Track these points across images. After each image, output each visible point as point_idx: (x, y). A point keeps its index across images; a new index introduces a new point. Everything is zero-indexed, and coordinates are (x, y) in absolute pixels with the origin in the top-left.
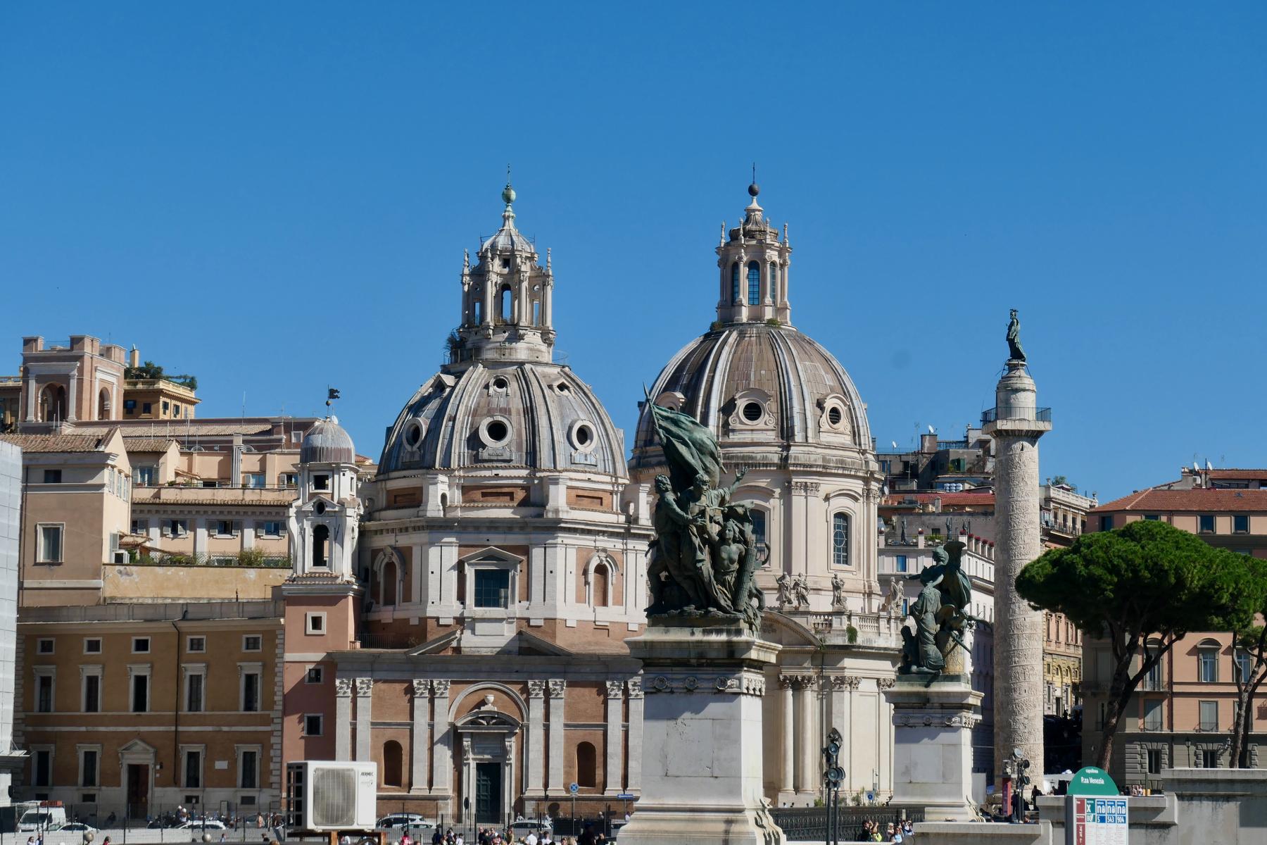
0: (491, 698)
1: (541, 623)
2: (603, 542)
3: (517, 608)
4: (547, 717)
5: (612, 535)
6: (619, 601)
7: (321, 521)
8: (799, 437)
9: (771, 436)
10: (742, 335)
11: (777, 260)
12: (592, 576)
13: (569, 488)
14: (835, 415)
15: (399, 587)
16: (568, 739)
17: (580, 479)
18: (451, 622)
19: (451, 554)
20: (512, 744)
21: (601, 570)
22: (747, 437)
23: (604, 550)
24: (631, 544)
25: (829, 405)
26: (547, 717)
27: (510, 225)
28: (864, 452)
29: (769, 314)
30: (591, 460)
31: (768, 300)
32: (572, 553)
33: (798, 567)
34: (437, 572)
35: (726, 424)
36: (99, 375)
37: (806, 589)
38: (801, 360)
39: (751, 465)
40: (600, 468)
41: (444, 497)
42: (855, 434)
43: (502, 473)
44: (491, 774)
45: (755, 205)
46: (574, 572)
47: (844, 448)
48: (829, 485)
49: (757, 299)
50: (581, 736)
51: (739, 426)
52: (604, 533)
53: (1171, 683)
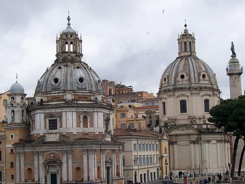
2: (85, 110)
4: (67, 160)
5: (89, 107)
6: (92, 125)
7: (13, 109)
9: (187, 82)
11: (191, 41)
12: (82, 120)
13: (75, 95)
14: (204, 76)
15: (34, 126)
18: (42, 135)
19: (42, 116)
21: (85, 118)
22: (181, 83)
23: (86, 112)
25: (202, 74)
26: (67, 160)
28: (212, 84)
29: (189, 54)
30: (84, 87)
32: (74, 114)
34: (39, 121)
36: (108, 87)
37: (195, 119)
39: (181, 89)
40: (87, 89)
41: (42, 100)
42: (209, 80)
46: (76, 119)
47: (206, 84)
48: (202, 93)
49: (186, 51)
50: (76, 166)
52: (85, 107)
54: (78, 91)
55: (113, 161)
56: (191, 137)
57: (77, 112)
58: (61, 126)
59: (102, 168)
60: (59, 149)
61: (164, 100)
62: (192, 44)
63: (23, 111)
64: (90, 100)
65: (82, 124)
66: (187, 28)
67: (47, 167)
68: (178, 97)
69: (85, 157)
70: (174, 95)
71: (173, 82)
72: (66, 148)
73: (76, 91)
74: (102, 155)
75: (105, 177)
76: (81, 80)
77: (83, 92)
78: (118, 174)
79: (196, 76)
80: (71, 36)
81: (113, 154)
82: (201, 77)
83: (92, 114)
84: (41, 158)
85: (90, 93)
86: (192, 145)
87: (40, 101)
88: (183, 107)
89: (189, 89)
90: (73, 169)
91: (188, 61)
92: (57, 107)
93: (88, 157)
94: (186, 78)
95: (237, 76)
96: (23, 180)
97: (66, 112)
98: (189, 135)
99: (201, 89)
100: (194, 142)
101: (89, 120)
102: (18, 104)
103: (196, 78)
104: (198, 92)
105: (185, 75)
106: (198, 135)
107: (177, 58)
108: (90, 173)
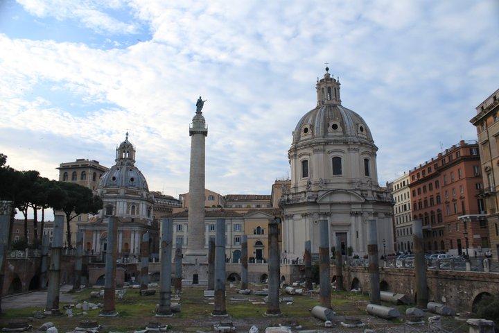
9: (341, 134)
22: (334, 134)
56: (353, 206)
66: (329, 72)
68: (329, 153)
70: (324, 150)
82: (359, 130)
86: (353, 218)
88: (337, 165)
89: (346, 143)
94: (340, 128)
98: (350, 204)
100: (356, 214)
104: (357, 147)
105: (338, 124)
106: (363, 204)
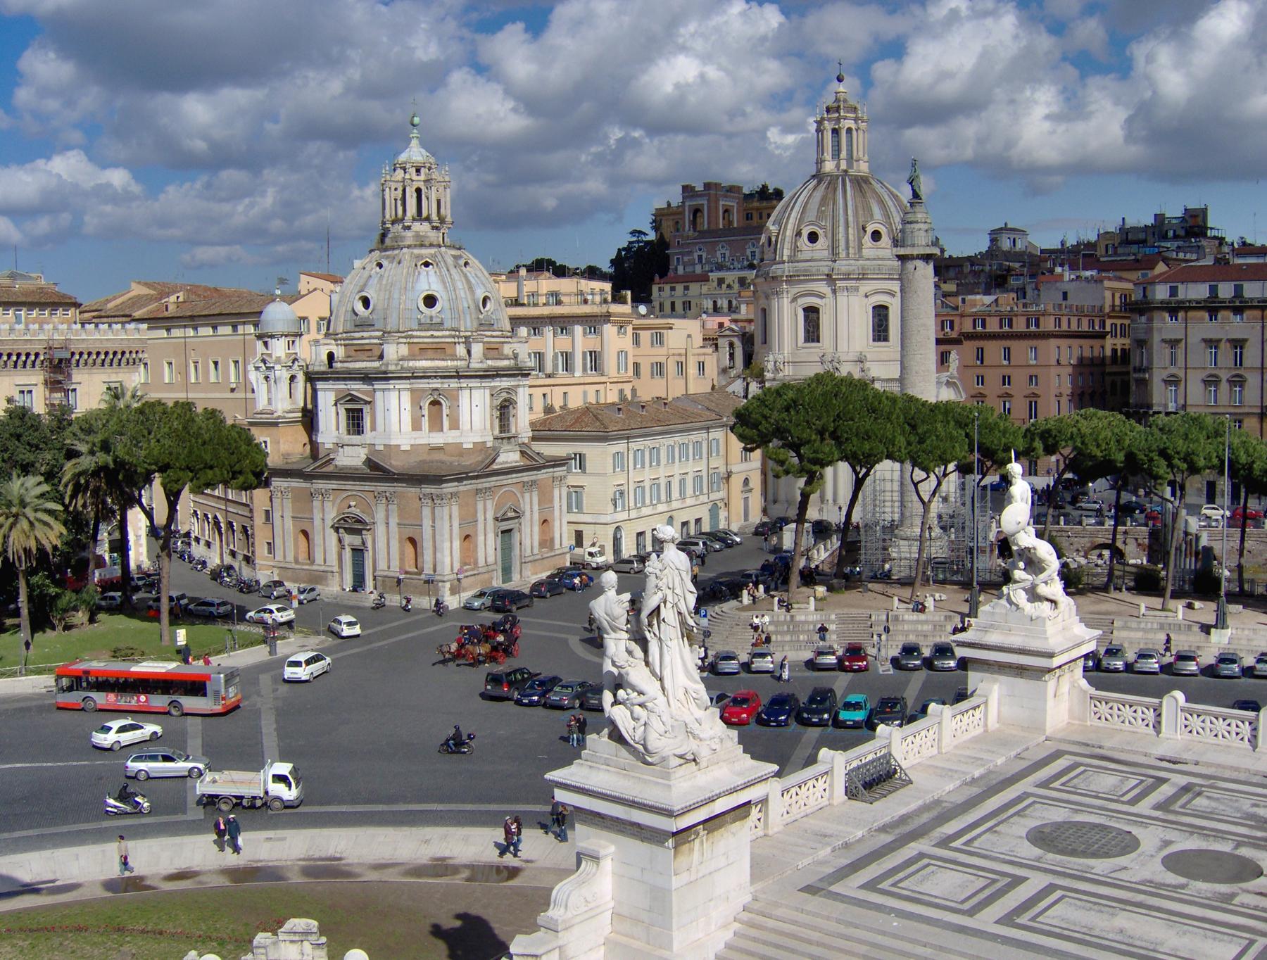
0: (353, 503)
1: (381, 448)
2: (436, 384)
3: (368, 436)
8: (843, 255)
9: (825, 254)
10: (819, 183)
11: (853, 126)
14: (876, 236)
16: (400, 533)
17: (424, 337)
18: (331, 446)
20: (368, 537)
21: (435, 403)
23: (436, 389)
24: (464, 383)
27: (414, 142)
29: (843, 166)
31: (844, 154)
32: (406, 397)
33: (843, 346)
35: (796, 249)
36: (721, 203)
38: (854, 197)
40: (447, 324)
43: (365, 334)
44: (358, 553)
45: (841, 89)
48: (866, 287)
50: (409, 532)
51: (805, 248)
53: (1184, 407)
54: (418, 333)
55: (528, 514)
57: (412, 391)
58: (373, 429)
59: (481, 538)
60: (367, 488)
61: (763, 303)
62: (854, 133)
63: (293, 378)
64: (454, 357)
65: (425, 423)
67: (341, 531)
69: (426, 512)
71: (786, 252)
72: (382, 487)
73: (415, 333)
74: (480, 506)
75: (491, 559)
76: (430, 301)
77: (432, 336)
78: (547, 542)
79: (851, 237)
80: (418, 171)
81: (527, 495)
83: (453, 396)
84: (328, 505)
85: (454, 337)
87: (325, 358)
90: (400, 542)
91: (835, 189)
92: (367, 378)
93: (433, 513)
94: (822, 242)
95: (919, 263)
96: (290, 558)
97: (383, 390)
99: (863, 277)
101: (445, 411)
102: (278, 360)
103: (851, 244)
105: (820, 232)
107: (813, 177)
108: (438, 555)
